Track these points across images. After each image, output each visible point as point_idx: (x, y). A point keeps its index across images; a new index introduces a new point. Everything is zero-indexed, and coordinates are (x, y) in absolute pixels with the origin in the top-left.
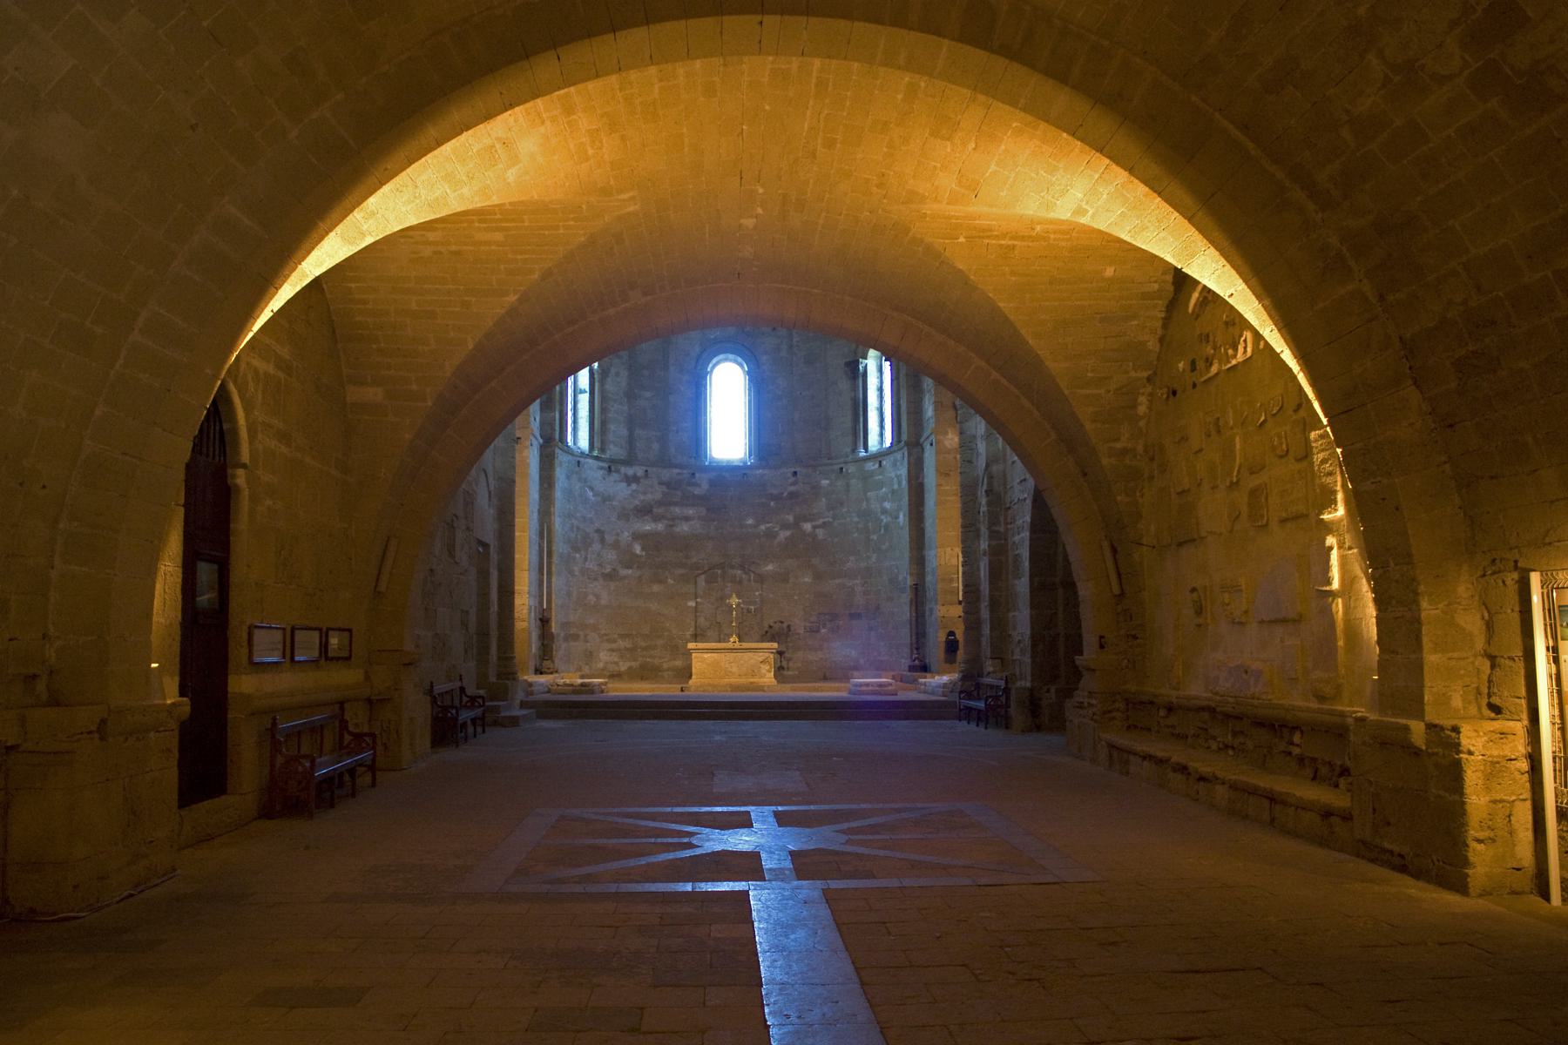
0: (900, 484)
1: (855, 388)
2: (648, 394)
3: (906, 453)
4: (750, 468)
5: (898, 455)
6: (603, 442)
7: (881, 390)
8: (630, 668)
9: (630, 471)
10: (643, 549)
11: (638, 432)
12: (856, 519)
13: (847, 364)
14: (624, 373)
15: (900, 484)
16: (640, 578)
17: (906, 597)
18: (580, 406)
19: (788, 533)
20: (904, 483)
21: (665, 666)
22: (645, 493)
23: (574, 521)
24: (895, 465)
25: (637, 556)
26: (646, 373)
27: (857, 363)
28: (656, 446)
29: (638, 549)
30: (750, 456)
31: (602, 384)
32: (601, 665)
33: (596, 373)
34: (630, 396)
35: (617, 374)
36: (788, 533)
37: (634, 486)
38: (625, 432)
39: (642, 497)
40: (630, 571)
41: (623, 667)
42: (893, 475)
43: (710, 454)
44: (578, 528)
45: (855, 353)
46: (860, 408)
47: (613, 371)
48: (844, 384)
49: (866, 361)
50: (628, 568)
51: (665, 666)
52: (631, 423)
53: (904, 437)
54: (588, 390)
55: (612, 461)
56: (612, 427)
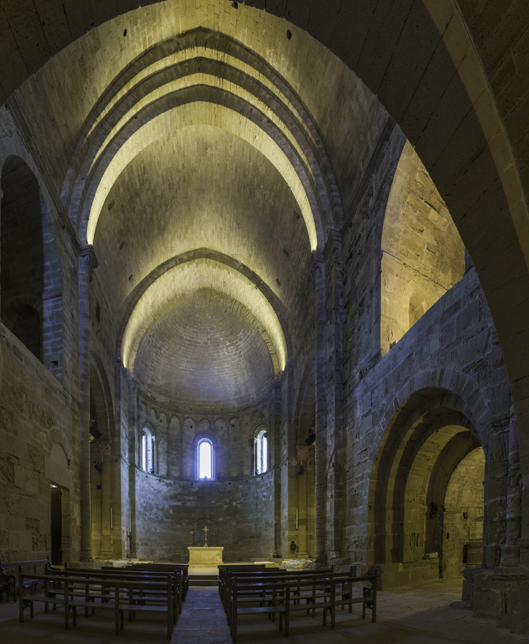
0: (270, 484)
3: (274, 472)
4: (214, 481)
5: (270, 473)
8: (169, 556)
9: (168, 482)
10: (173, 512)
12: (253, 500)
15: (270, 484)
16: (172, 522)
17: (273, 529)
19: (227, 506)
20: (273, 484)
21: (182, 556)
22: (174, 490)
23: (146, 500)
24: (268, 477)
25: (171, 514)
27: (253, 439)
29: (171, 512)
32: (157, 555)
34: (168, 452)
36: (227, 506)
37: (170, 487)
39: (173, 492)
40: (169, 520)
41: (166, 556)
42: (268, 481)
44: (147, 502)
50: (168, 518)
51: (182, 556)
53: (273, 465)
55: (161, 477)
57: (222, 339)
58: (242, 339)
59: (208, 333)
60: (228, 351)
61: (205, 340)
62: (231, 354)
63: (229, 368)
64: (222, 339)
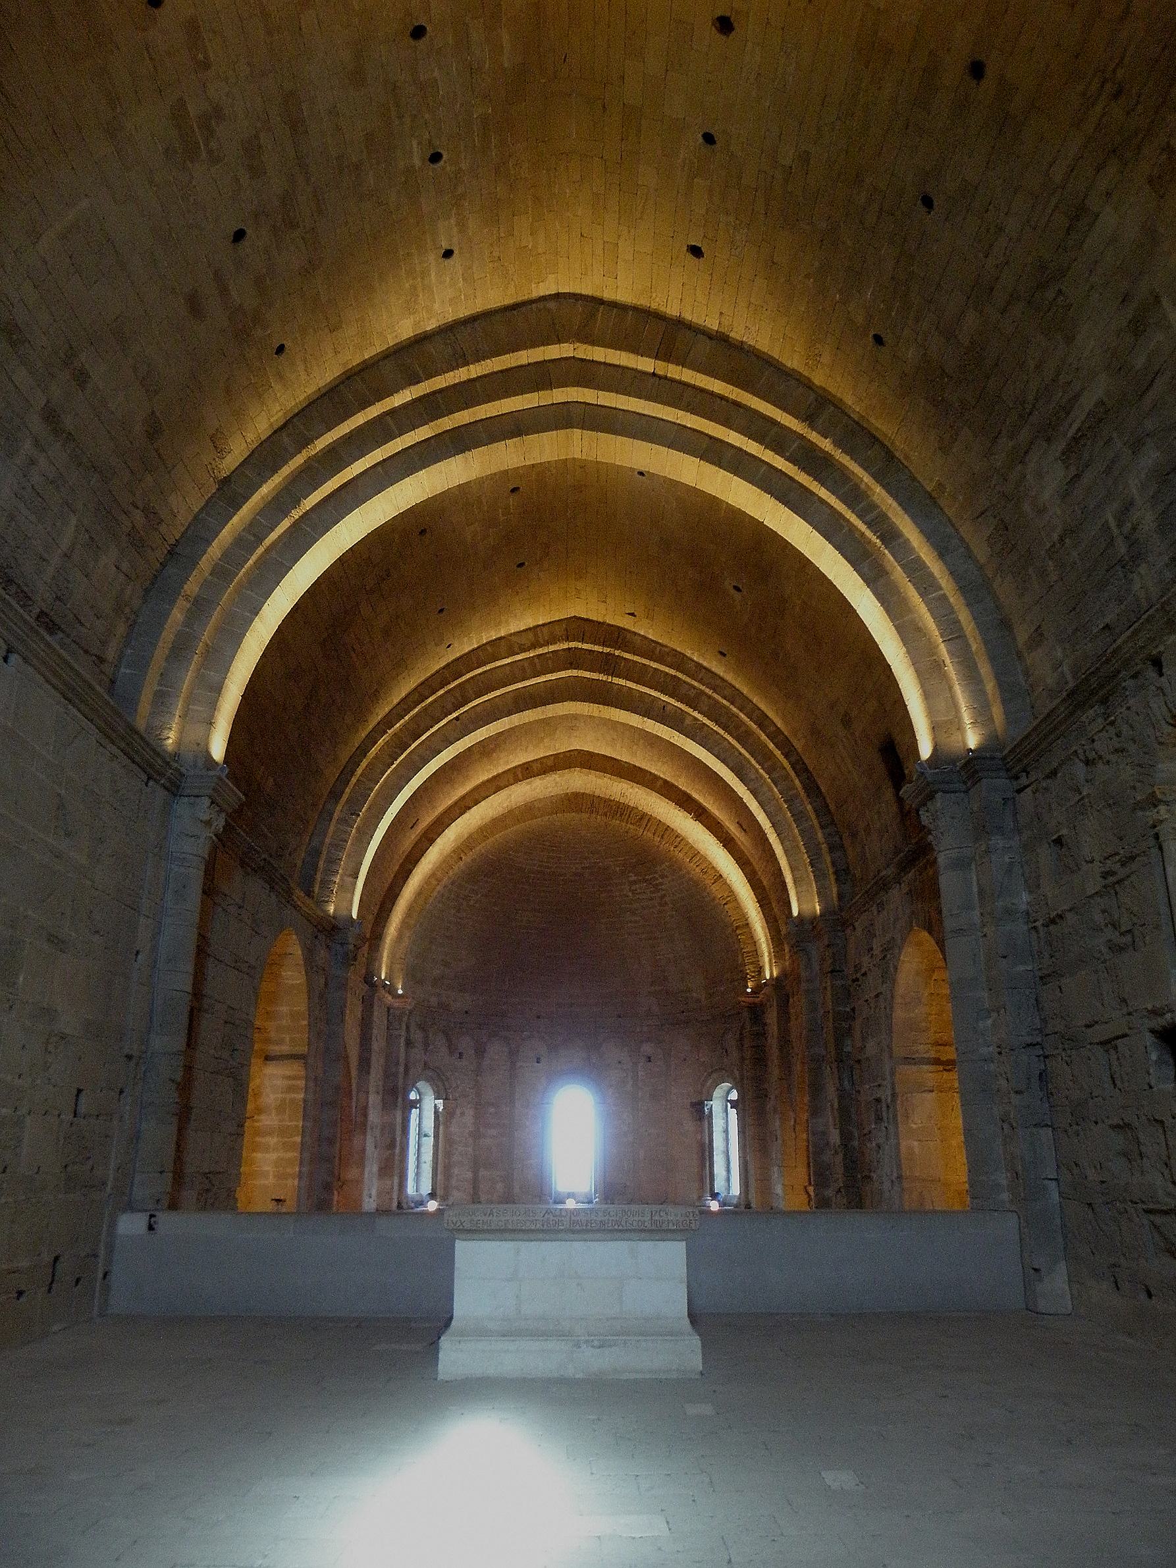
1: (702, 1132)
2: (493, 1132)
6: (447, 1188)
7: (726, 1131)
11: (483, 1172)
13: (693, 1105)
14: (470, 1113)
18: (423, 1150)
26: (492, 1110)
28: (500, 1186)
30: (595, 1193)
31: (447, 1127)
33: (440, 1115)
35: (463, 1114)
38: (469, 1175)
43: (555, 1188)
45: (701, 1093)
46: (705, 1152)
47: (458, 1112)
48: (689, 1125)
49: (711, 1102)
52: (476, 1165)
54: (431, 1132)
56: (456, 1171)
57: (618, 869)
58: (667, 877)
59: (586, 858)
60: (633, 892)
61: (576, 868)
62: (641, 897)
63: (636, 922)
64: (618, 869)
